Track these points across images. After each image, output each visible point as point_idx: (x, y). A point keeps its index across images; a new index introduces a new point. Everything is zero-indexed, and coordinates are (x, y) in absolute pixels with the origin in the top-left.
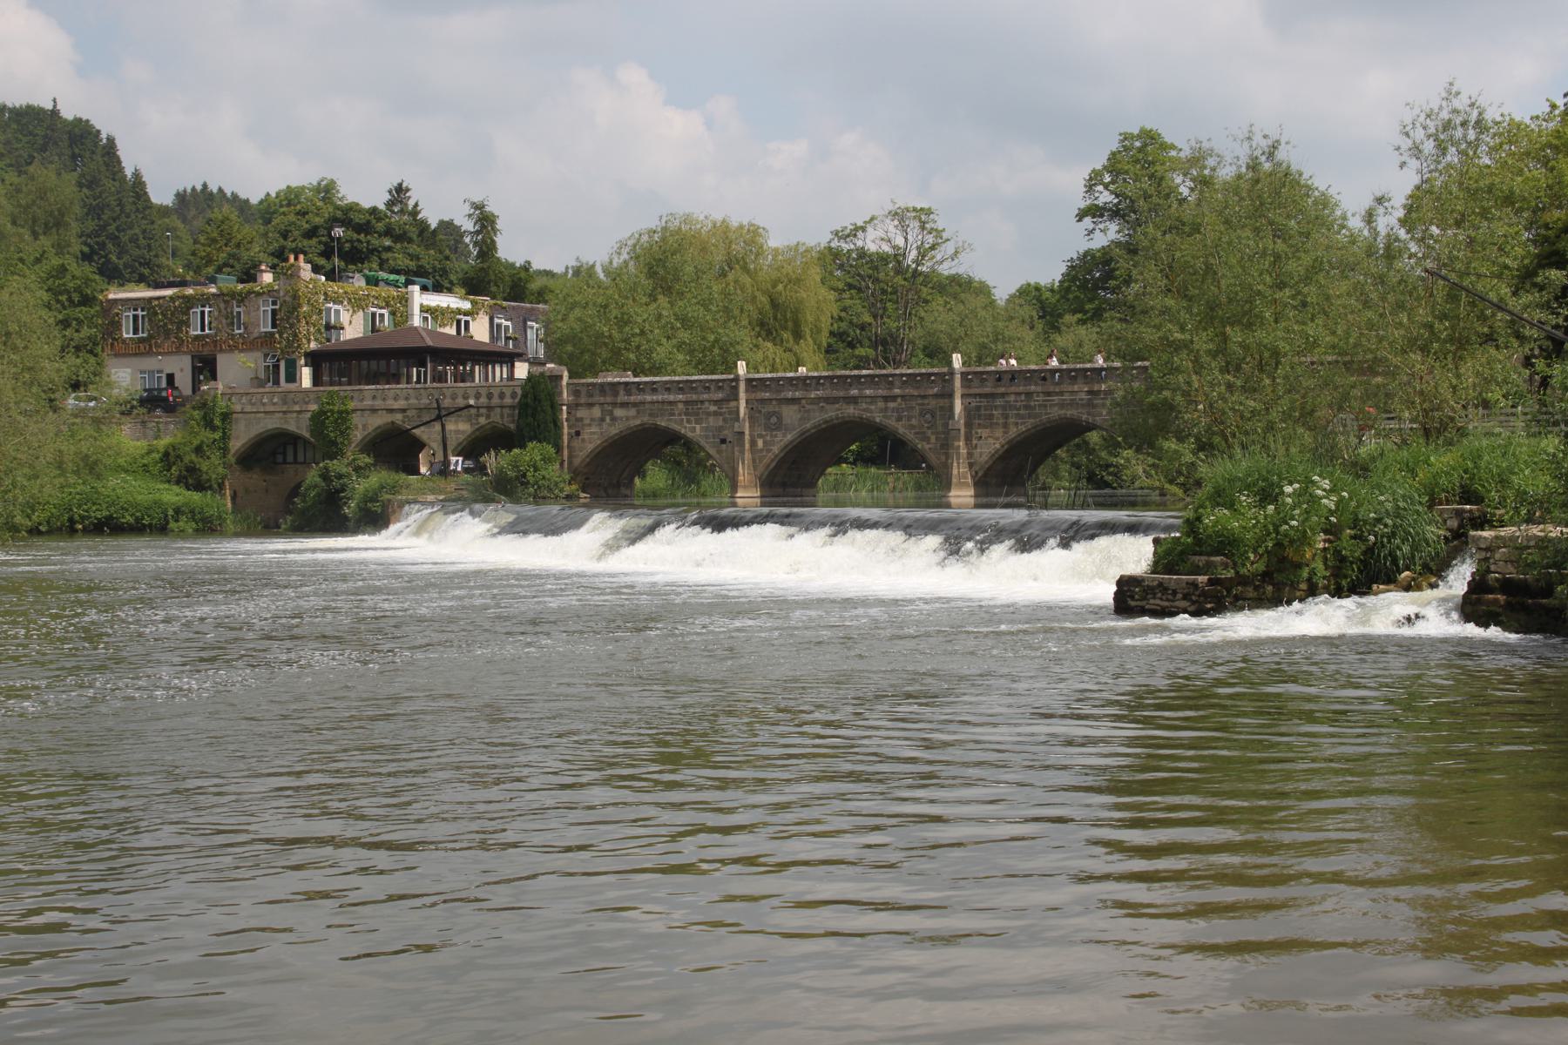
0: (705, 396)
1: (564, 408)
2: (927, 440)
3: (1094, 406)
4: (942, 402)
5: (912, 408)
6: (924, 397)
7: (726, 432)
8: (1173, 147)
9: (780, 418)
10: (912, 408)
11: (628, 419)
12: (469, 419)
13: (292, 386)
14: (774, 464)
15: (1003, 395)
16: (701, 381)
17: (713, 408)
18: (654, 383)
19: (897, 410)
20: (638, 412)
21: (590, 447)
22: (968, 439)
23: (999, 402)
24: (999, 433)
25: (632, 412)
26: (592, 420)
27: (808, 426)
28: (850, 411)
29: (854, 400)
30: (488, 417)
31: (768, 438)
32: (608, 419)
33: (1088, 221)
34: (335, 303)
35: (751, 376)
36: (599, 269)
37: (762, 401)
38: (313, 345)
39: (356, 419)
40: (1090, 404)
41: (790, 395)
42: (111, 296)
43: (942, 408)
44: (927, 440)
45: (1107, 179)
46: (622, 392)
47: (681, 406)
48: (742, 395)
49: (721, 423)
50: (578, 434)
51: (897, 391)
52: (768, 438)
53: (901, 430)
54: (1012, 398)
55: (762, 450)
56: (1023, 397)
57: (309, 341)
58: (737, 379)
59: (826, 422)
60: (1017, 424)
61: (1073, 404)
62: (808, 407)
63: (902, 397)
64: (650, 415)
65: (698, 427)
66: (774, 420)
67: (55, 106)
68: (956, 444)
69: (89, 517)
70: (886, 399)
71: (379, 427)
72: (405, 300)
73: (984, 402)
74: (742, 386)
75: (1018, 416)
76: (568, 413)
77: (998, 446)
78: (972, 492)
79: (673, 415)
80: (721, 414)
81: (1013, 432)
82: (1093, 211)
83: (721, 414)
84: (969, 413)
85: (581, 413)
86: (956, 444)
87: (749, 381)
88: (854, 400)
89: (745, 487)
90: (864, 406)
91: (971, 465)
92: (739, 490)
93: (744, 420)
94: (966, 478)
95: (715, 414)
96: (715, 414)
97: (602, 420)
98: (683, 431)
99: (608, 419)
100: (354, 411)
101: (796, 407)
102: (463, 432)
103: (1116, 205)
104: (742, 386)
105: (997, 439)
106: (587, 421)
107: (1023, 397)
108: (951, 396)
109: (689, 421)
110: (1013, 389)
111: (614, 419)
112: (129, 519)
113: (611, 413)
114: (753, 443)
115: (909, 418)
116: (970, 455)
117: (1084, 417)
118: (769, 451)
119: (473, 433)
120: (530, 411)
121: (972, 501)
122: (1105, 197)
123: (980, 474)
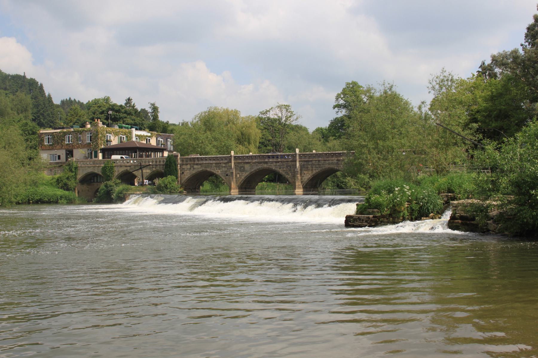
0: (221, 162)
1: (179, 165)
2: (288, 174)
3: (339, 164)
4: (293, 163)
5: (284, 165)
6: (287, 162)
7: (228, 172)
8: (362, 87)
9: (244, 168)
10: (284, 165)
11: (198, 168)
12: (150, 169)
13: (96, 159)
14: (242, 182)
15: (311, 161)
16: (220, 157)
17: (224, 165)
18: (206, 158)
20: (201, 166)
21: (187, 177)
22: (301, 174)
23: (310, 163)
24: (310, 172)
25: (199, 166)
26: (187, 169)
27: (253, 170)
28: (265, 166)
29: (266, 163)
30: (156, 168)
31: (241, 174)
32: (192, 168)
33: (336, 109)
34: (109, 134)
35: (235, 155)
36: (189, 123)
37: (239, 163)
38: (103, 147)
39: (116, 169)
40: (337, 164)
41: (247, 161)
42: (41, 132)
43: (293, 165)
44: (288, 174)
45: (342, 96)
46: (196, 160)
47: (214, 164)
48: (233, 161)
49: (226, 170)
50: (183, 173)
51: (279, 160)
52: (241, 174)
53: (281, 172)
54: (314, 162)
55: (238, 178)
56: (317, 162)
57: (101, 145)
58: (231, 156)
59: (258, 169)
60: (315, 170)
61: (332, 164)
62: (252, 165)
64: (205, 167)
65: (219, 171)
66: (242, 169)
67: (24, 75)
68: (297, 176)
69: (34, 199)
70: (276, 162)
71: (123, 171)
72: (130, 133)
73: (306, 163)
74: (233, 159)
75: (316, 167)
76: (180, 167)
77: (310, 176)
78: (302, 190)
79: (212, 167)
80: (226, 167)
81: (314, 172)
82: (338, 106)
83: (226, 167)
84: (302, 167)
85: (184, 167)
86: (297, 176)
87: (235, 157)
88: (266, 163)
89: (234, 189)
90: (270, 164)
91: (302, 182)
92: (232, 190)
93: (233, 169)
94: (300, 186)
95: (225, 167)
96: (225, 167)
97: (190, 169)
98: (215, 172)
99: (192, 168)
100: (115, 166)
101: (249, 165)
102: (148, 173)
103: (345, 104)
104: (233, 159)
105: (310, 174)
106: (186, 169)
107: (317, 162)
108: (295, 161)
109: (216, 169)
110: (314, 159)
111: (194, 169)
112: (46, 199)
113: (193, 167)
114: (236, 176)
115: (283, 168)
116: (301, 179)
117: (336, 168)
118: (241, 178)
119: (151, 173)
120: (168, 166)
121: (302, 193)
122: (342, 102)
123: (304, 185)
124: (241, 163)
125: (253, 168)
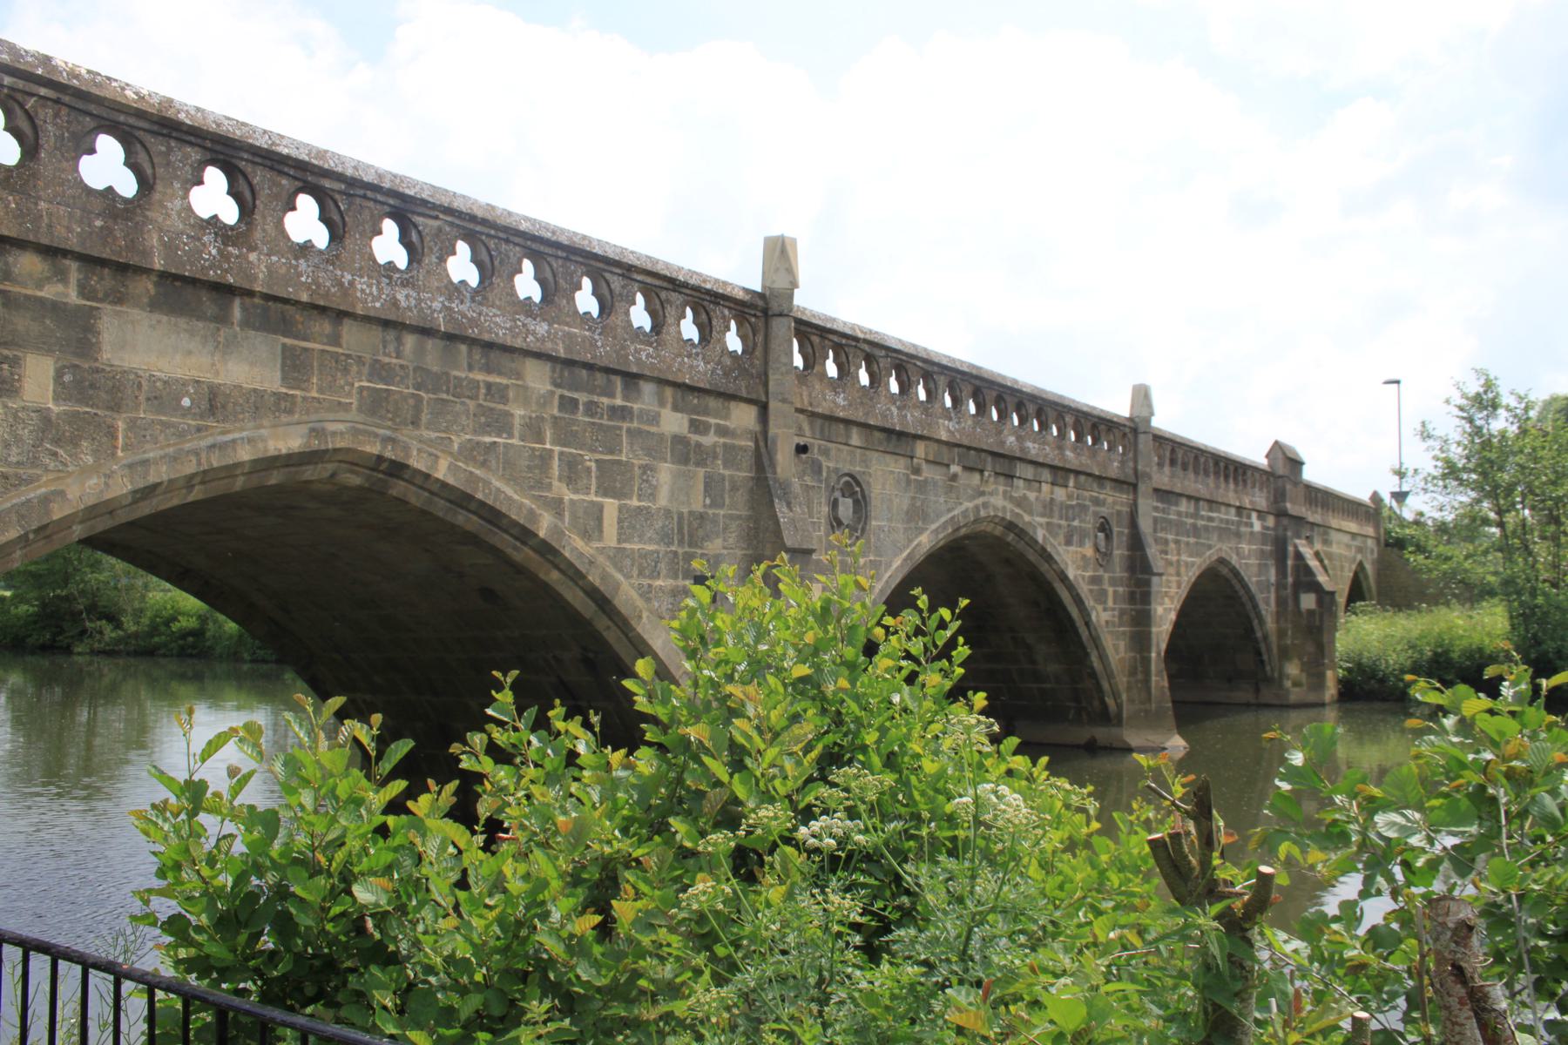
10: (1084, 508)
11: (214, 402)
17: (673, 422)
19: (1067, 511)
29: (1006, 464)
49: (698, 502)
63: (1077, 473)
65: (611, 506)
79: (501, 424)
98: (544, 527)
101: (898, 466)
124: (847, 422)
125: (925, 518)
